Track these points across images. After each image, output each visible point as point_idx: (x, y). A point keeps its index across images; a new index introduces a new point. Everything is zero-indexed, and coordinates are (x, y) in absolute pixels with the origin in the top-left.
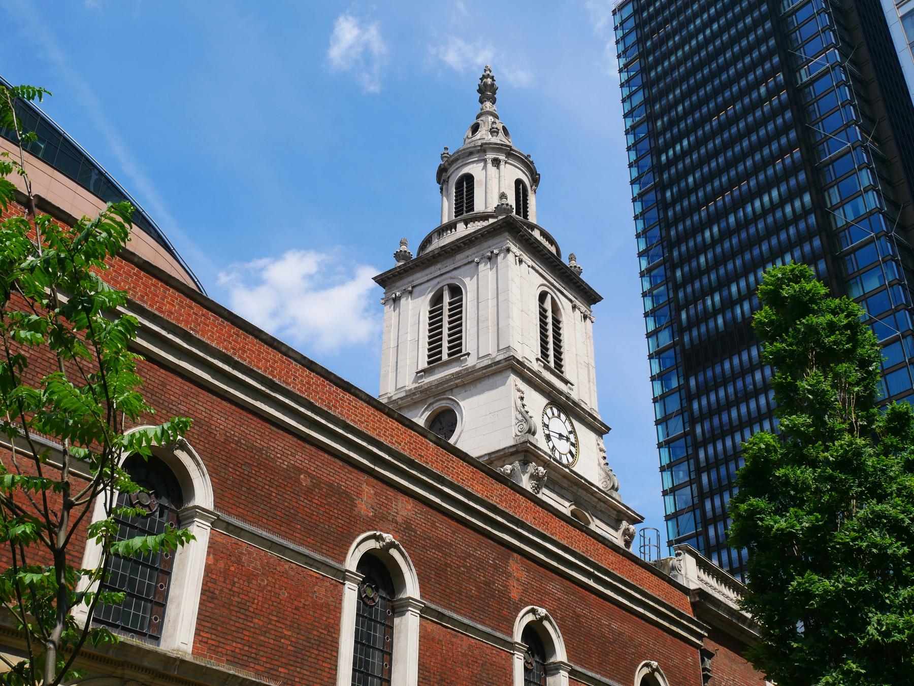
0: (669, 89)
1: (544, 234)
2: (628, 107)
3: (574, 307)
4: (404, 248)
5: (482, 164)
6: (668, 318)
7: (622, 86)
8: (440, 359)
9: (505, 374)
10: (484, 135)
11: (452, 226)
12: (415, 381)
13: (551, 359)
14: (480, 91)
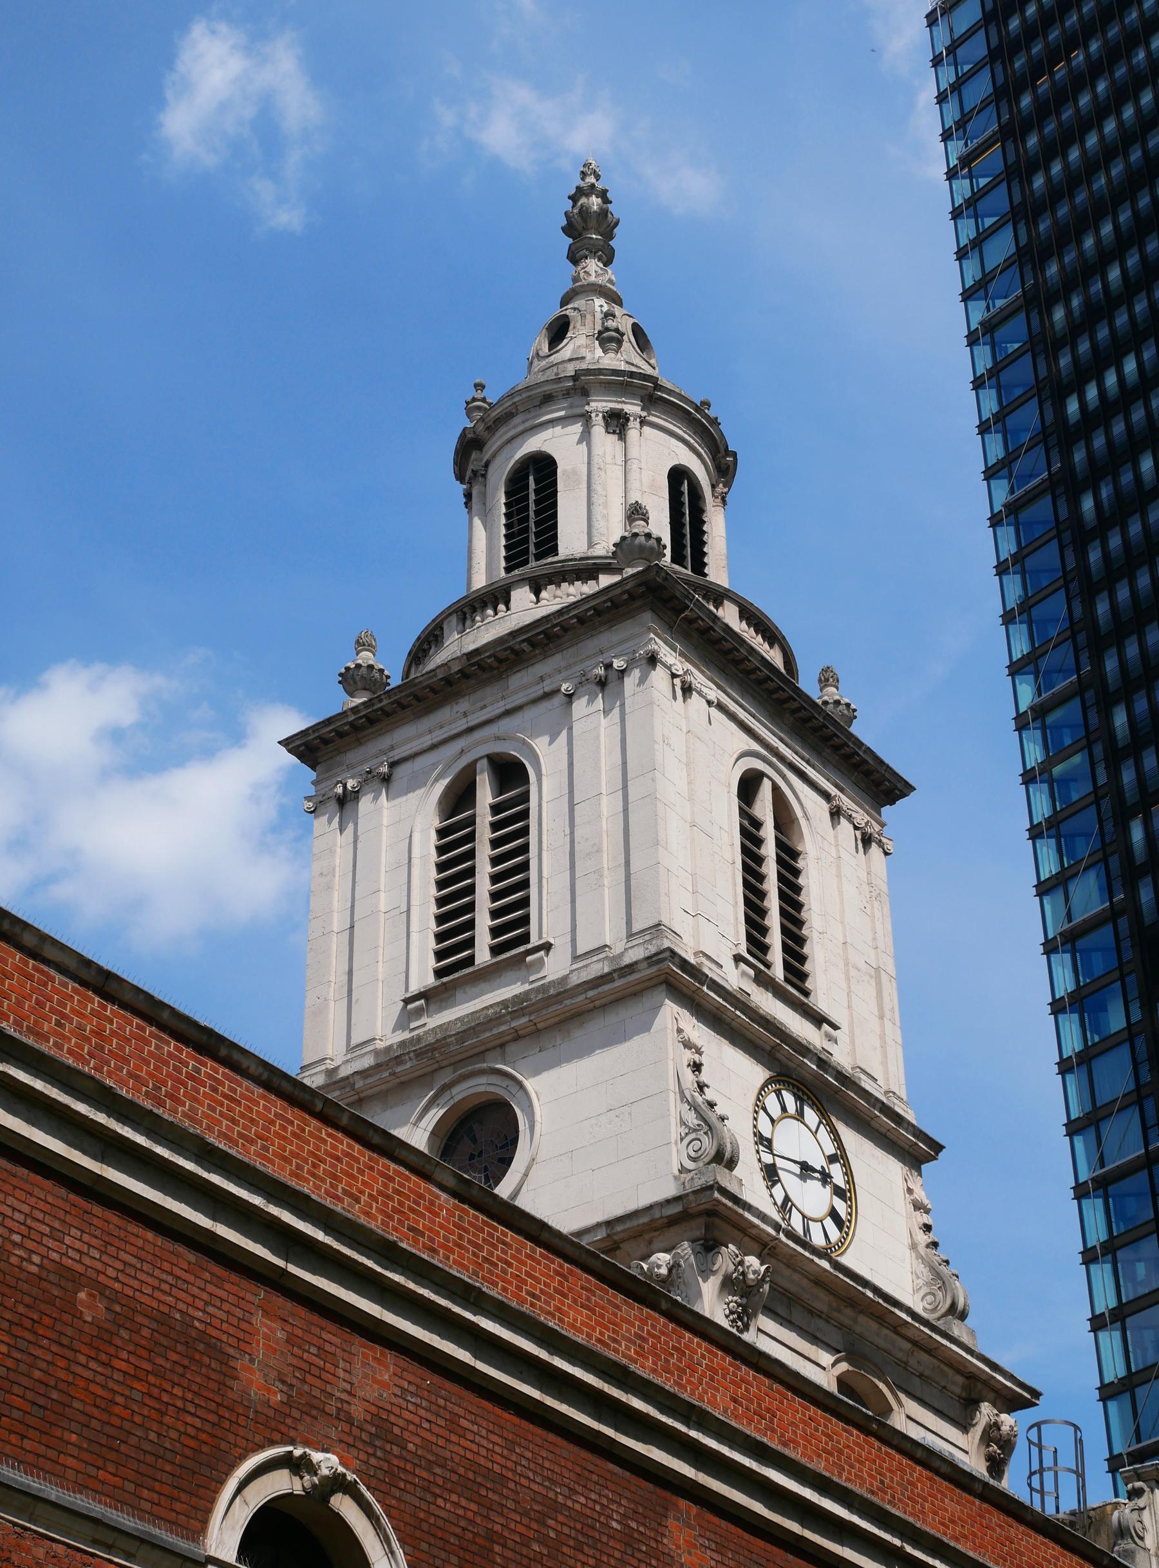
0: (1086, 221)
1: (748, 613)
2: (973, 272)
3: (836, 814)
4: (366, 658)
5: (577, 428)
6: (1094, 842)
7: (956, 214)
8: (470, 960)
9: (648, 1000)
10: (581, 349)
11: (497, 596)
12: (402, 1023)
13: (776, 956)
14: (570, 229)
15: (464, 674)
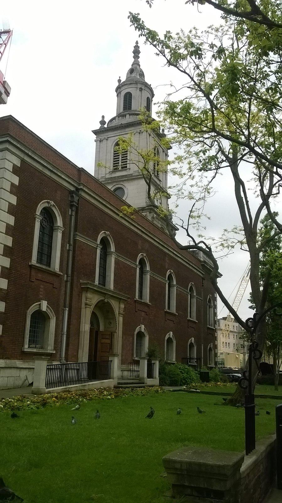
15: (120, 127)
